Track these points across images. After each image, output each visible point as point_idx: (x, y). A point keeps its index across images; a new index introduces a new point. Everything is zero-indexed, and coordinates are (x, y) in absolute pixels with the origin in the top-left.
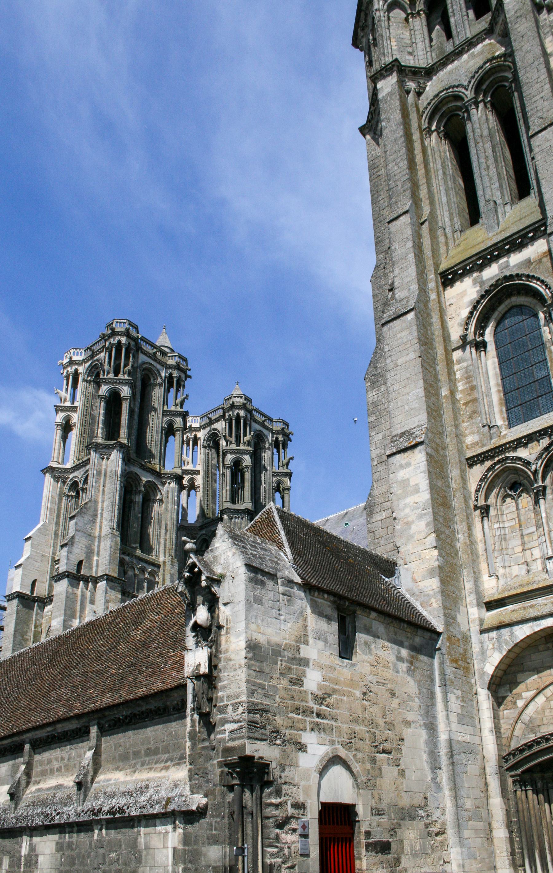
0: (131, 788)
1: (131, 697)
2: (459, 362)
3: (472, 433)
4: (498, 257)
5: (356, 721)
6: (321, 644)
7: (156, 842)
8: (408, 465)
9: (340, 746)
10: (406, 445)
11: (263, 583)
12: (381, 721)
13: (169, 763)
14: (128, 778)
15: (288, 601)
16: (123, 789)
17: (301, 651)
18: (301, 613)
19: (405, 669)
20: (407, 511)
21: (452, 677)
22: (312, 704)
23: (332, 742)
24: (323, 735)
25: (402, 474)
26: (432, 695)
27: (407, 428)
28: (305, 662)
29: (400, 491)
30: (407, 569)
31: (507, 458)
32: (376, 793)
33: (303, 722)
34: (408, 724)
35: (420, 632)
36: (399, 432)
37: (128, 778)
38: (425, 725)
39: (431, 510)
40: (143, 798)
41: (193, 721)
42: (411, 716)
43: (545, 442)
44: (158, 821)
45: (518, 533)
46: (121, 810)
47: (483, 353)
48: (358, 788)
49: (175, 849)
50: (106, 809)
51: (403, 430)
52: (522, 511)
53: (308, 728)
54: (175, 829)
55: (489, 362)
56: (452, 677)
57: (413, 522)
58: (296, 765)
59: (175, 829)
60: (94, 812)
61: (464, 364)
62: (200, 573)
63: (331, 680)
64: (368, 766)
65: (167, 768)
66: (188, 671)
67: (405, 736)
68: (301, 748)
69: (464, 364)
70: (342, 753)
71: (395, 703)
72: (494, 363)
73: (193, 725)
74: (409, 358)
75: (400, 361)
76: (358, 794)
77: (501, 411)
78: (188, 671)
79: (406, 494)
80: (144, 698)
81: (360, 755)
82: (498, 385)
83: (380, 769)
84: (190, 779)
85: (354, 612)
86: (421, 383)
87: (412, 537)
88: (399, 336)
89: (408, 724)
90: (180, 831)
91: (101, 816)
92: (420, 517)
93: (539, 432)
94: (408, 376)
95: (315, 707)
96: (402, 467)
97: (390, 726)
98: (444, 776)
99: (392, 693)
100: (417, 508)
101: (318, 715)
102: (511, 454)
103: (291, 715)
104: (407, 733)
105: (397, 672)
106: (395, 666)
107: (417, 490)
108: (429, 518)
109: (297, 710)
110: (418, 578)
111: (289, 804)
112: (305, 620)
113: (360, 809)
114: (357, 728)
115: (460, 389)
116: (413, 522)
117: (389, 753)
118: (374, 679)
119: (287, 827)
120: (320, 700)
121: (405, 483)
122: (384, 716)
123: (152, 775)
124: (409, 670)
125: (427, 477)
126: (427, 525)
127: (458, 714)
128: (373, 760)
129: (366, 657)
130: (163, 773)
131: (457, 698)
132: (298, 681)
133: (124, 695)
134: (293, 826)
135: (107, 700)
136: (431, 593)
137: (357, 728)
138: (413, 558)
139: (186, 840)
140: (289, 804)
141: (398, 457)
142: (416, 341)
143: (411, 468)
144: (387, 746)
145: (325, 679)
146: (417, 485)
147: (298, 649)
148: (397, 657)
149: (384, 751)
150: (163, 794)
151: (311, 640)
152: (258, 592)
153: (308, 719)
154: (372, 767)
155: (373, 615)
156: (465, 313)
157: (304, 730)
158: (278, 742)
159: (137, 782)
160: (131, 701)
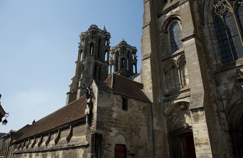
0: (76, 140)
1: (77, 119)
2: (161, 36)
3: (163, 54)
4: (170, 10)
5: (127, 125)
7: (80, 152)
8: (146, 62)
10: (146, 57)
12: (134, 125)
13: (84, 134)
14: (76, 138)
16: (75, 140)
17: (112, 109)
19: (141, 112)
20: (146, 73)
21: (155, 114)
25: (145, 64)
26: (149, 118)
27: (147, 53)
29: (144, 69)
30: (146, 88)
31: (171, 60)
34: (142, 125)
35: (146, 103)
36: (145, 54)
37: (76, 138)
39: (151, 73)
40: (78, 142)
41: (87, 125)
42: (142, 123)
43: (180, 56)
44: (80, 148)
45: (174, 78)
46: (74, 145)
47: (167, 34)
49: (83, 154)
50: (71, 145)
51: (146, 54)
52: (175, 73)
54: (83, 149)
55: (168, 36)
56: (155, 114)
57: (147, 76)
59: (83, 149)
60: (69, 146)
61: (162, 37)
62: (88, 91)
64: (129, 136)
65: (83, 135)
66: (86, 113)
69: (162, 37)
71: (138, 120)
72: (169, 36)
73: (87, 126)
74: (147, 36)
75: (146, 37)
76: (127, 142)
77: (171, 48)
78: (86, 113)
79: (146, 70)
80: (79, 119)
81: (127, 133)
82: (170, 42)
83: (133, 136)
84: (86, 138)
85: (127, 99)
86: (150, 42)
87: (147, 80)
88: (146, 31)
89: (142, 125)
90: (84, 150)
91: (70, 147)
92: (149, 75)
93: (178, 53)
94: (147, 41)
96: (145, 63)
97: (136, 126)
99: (137, 118)
100: (148, 73)
102: (171, 59)
104: (142, 128)
105: (139, 113)
106: (138, 111)
107: (148, 68)
108: (151, 75)
110: (148, 89)
114: (127, 126)
115: (161, 43)
116: (147, 76)
117: (136, 132)
118: (132, 115)
121: (146, 66)
123: (81, 137)
125: (150, 65)
126: (150, 77)
127: (156, 123)
128: (131, 134)
130: (82, 137)
131: (156, 119)
133: (76, 118)
135: (73, 120)
136: (151, 93)
137: (127, 126)
138: (147, 85)
139: (85, 152)
141: (144, 60)
142: (149, 32)
143: (147, 63)
144: (135, 131)
146: (148, 67)
148: (139, 109)
149: (134, 132)
150: (82, 141)
155: (133, 99)
156: (162, 24)
159: (77, 138)
160: (77, 120)
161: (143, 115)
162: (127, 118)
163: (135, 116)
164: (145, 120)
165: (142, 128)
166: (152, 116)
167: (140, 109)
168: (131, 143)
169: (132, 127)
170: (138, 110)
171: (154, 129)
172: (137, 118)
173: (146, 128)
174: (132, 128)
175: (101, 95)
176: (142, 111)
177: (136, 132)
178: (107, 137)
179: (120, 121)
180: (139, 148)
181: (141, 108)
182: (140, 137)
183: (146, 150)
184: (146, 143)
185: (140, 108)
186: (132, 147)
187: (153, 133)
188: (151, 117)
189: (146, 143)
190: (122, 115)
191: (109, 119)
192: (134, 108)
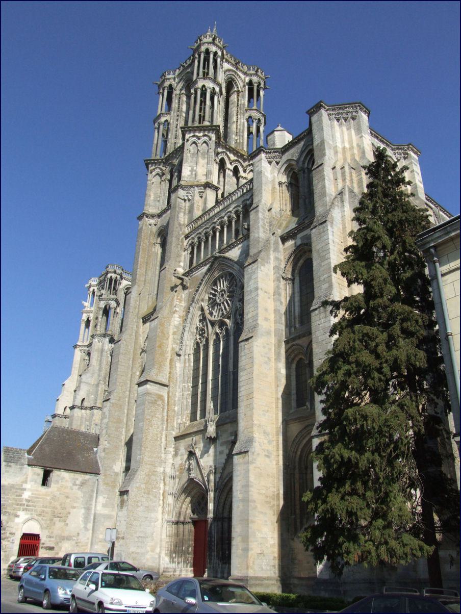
5: (46, 507)
6: (33, 483)
9: (35, 516)
11: (10, 466)
12: (58, 507)
15: (20, 470)
18: (26, 473)
22: (24, 502)
23: (31, 514)
24: (28, 512)
26: (91, 497)
28: (25, 489)
32: (50, 531)
33: (19, 508)
38: (85, 508)
42: (75, 505)
48: (42, 529)
53: (21, 510)
58: (13, 521)
63: (35, 494)
64: (49, 522)
67: (71, 512)
68: (17, 516)
70: (36, 517)
71: (68, 501)
76: (42, 531)
81: (44, 518)
83: (54, 523)
95: (26, 503)
97: (64, 508)
98: (90, 526)
101: (27, 506)
103: (14, 506)
105: (72, 489)
106: (71, 487)
109: (18, 504)
111: (8, 533)
112: (27, 476)
113: (41, 536)
114: (45, 509)
119: (6, 540)
120: (28, 501)
122: (61, 504)
124: (79, 489)
129: (55, 486)
131: (104, 498)
132: (20, 496)
134: (9, 539)
137: (45, 509)
140: (8, 533)
145: (32, 494)
147: (22, 485)
149: (58, 517)
151: (28, 482)
152: (7, 469)
153: (22, 507)
154: (50, 523)
157: (19, 510)
158: (7, 514)
161: (79, 492)
162: (48, 498)
163: (63, 494)
164: (82, 499)
165: (72, 511)
166: (97, 493)
167: (75, 484)
168: (49, 532)
169: (55, 511)
170: (71, 485)
171: (96, 512)
172: (67, 497)
173: (83, 511)
174: (54, 512)
175: (7, 469)
176: (78, 486)
177: (61, 517)
178: (10, 524)
179: (34, 503)
180: (63, 540)
181: (78, 482)
182: (67, 524)
183: (76, 543)
184: (78, 534)
185: (75, 482)
186: (50, 537)
187: (94, 519)
188: (95, 495)
189: (78, 534)
190: (39, 495)
191: (16, 501)
192: (63, 483)
